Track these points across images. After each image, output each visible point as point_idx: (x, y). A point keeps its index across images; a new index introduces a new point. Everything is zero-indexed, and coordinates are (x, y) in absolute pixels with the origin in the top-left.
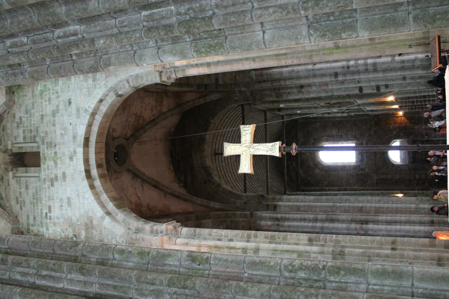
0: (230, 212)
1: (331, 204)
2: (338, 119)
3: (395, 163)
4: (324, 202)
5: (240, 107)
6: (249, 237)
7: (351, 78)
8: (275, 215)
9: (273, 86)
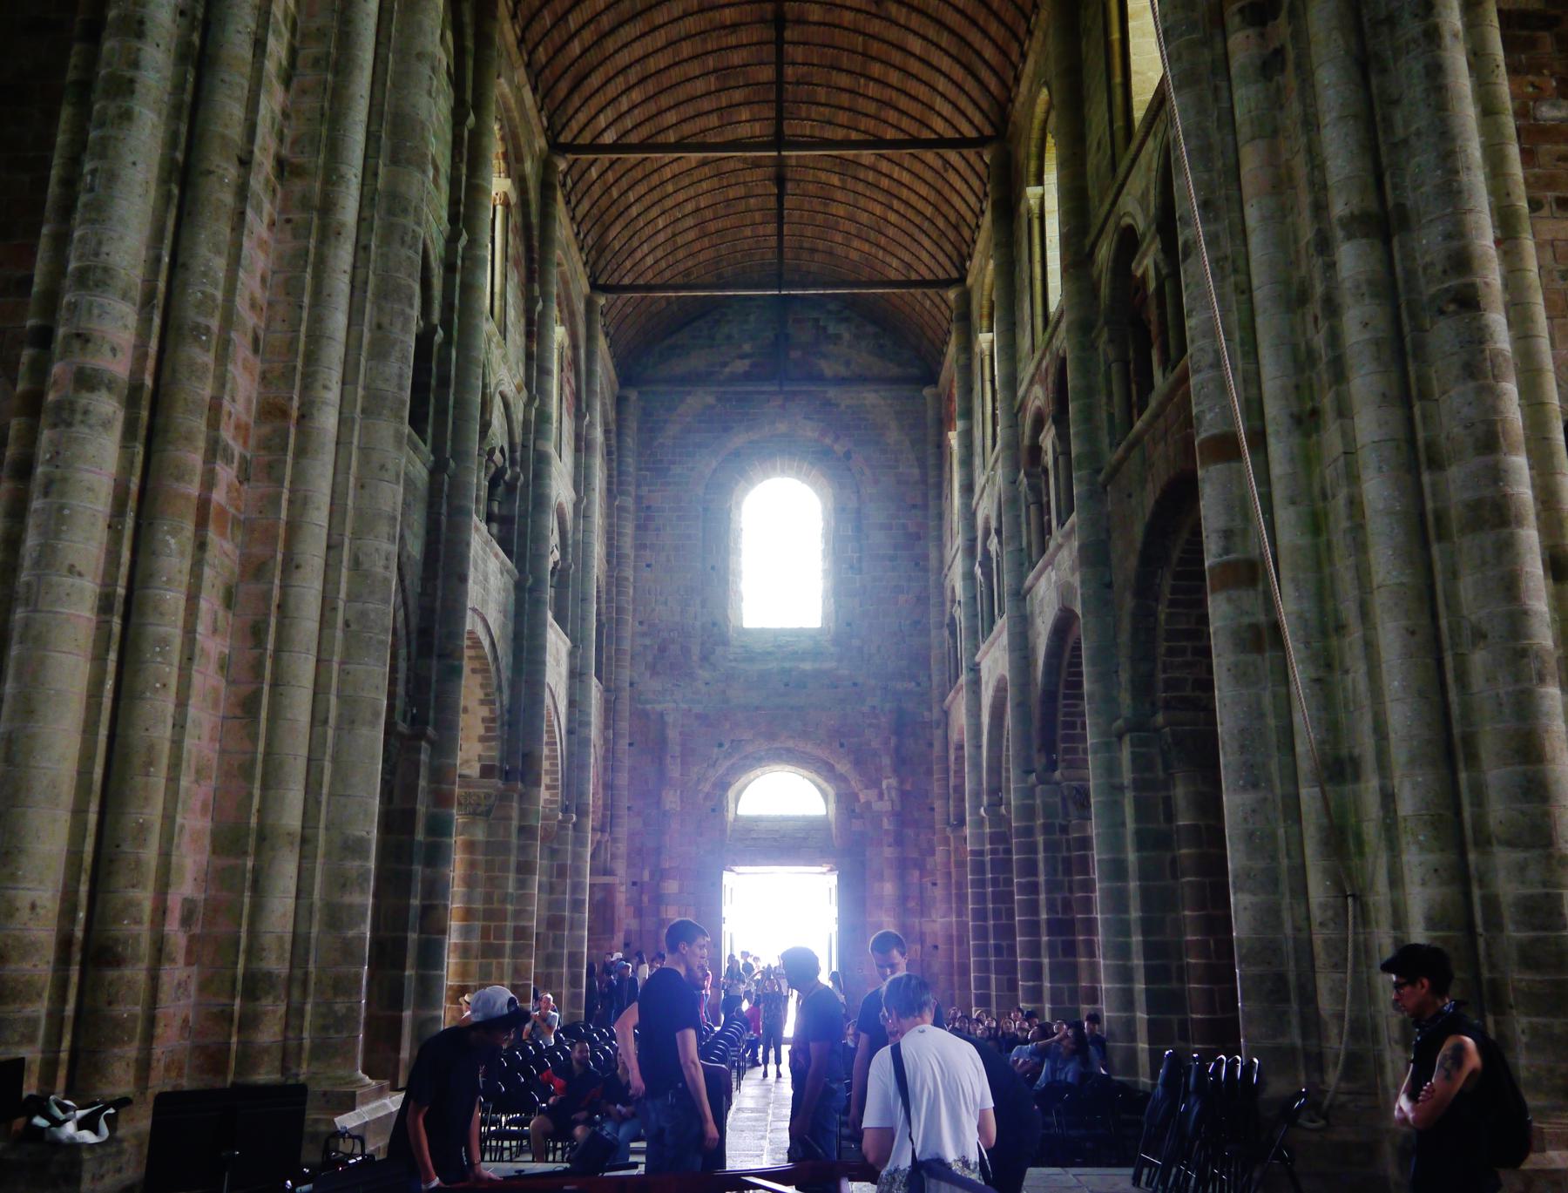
2: (933, 554)
3: (731, 794)
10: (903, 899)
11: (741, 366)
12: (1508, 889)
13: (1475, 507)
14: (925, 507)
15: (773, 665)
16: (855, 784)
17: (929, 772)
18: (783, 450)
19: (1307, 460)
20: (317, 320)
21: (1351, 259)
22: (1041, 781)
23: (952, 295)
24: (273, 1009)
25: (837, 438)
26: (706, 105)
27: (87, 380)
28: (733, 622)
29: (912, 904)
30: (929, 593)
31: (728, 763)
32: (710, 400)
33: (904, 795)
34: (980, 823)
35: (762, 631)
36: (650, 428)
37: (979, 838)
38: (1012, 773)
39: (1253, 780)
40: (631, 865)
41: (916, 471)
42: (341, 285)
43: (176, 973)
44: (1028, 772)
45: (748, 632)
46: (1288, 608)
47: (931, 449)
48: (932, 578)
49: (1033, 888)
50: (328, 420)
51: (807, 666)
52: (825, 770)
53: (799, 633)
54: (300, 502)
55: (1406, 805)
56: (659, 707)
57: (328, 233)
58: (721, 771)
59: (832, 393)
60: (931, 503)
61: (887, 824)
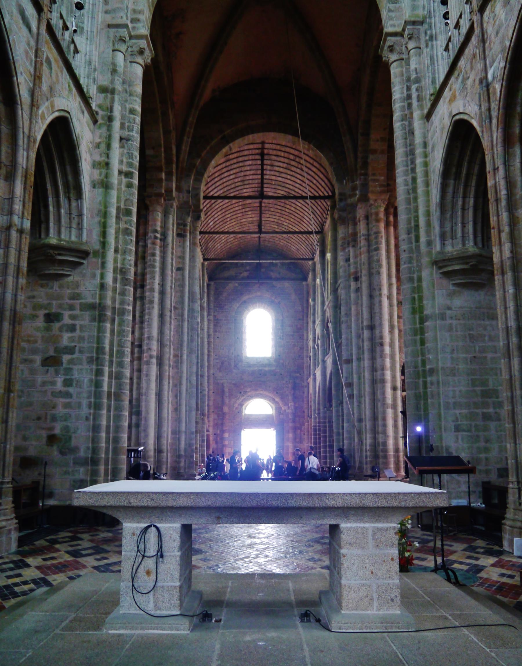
0: (174, 166)
1: (186, 316)
2: (305, 335)
3: (244, 407)
4: (189, 306)
5: (330, 194)
6: (128, 175)
7: (366, 348)
8: (170, 233)
9: (360, 237)
10: (295, 438)
11: (246, 274)
12: (381, 440)
13: (380, 380)
14: (303, 320)
15: (256, 369)
16: (281, 405)
17: (303, 401)
18: (260, 300)
19: (359, 367)
20: (182, 338)
21: (366, 334)
22: (328, 410)
23: (310, 263)
24: (183, 460)
25: (276, 298)
26: (238, 212)
27: (151, 357)
28: (244, 355)
29: (297, 440)
30: (303, 348)
31: (243, 398)
32: (236, 285)
33: (296, 408)
34: (315, 418)
35: (253, 358)
36: (218, 293)
37: (315, 422)
38: (321, 408)
39: (348, 422)
40: (214, 428)
41: (300, 308)
42: (186, 331)
43: (169, 454)
44: (325, 407)
45: (248, 358)
46: (355, 392)
47: (305, 302)
48: (305, 342)
49: (325, 437)
50: (185, 357)
51: (267, 369)
52: (273, 400)
53: (264, 358)
54: (181, 372)
55: (368, 427)
56: (222, 382)
57: (183, 320)
58: (241, 401)
59: (274, 283)
60: (305, 318)
61: (290, 416)
